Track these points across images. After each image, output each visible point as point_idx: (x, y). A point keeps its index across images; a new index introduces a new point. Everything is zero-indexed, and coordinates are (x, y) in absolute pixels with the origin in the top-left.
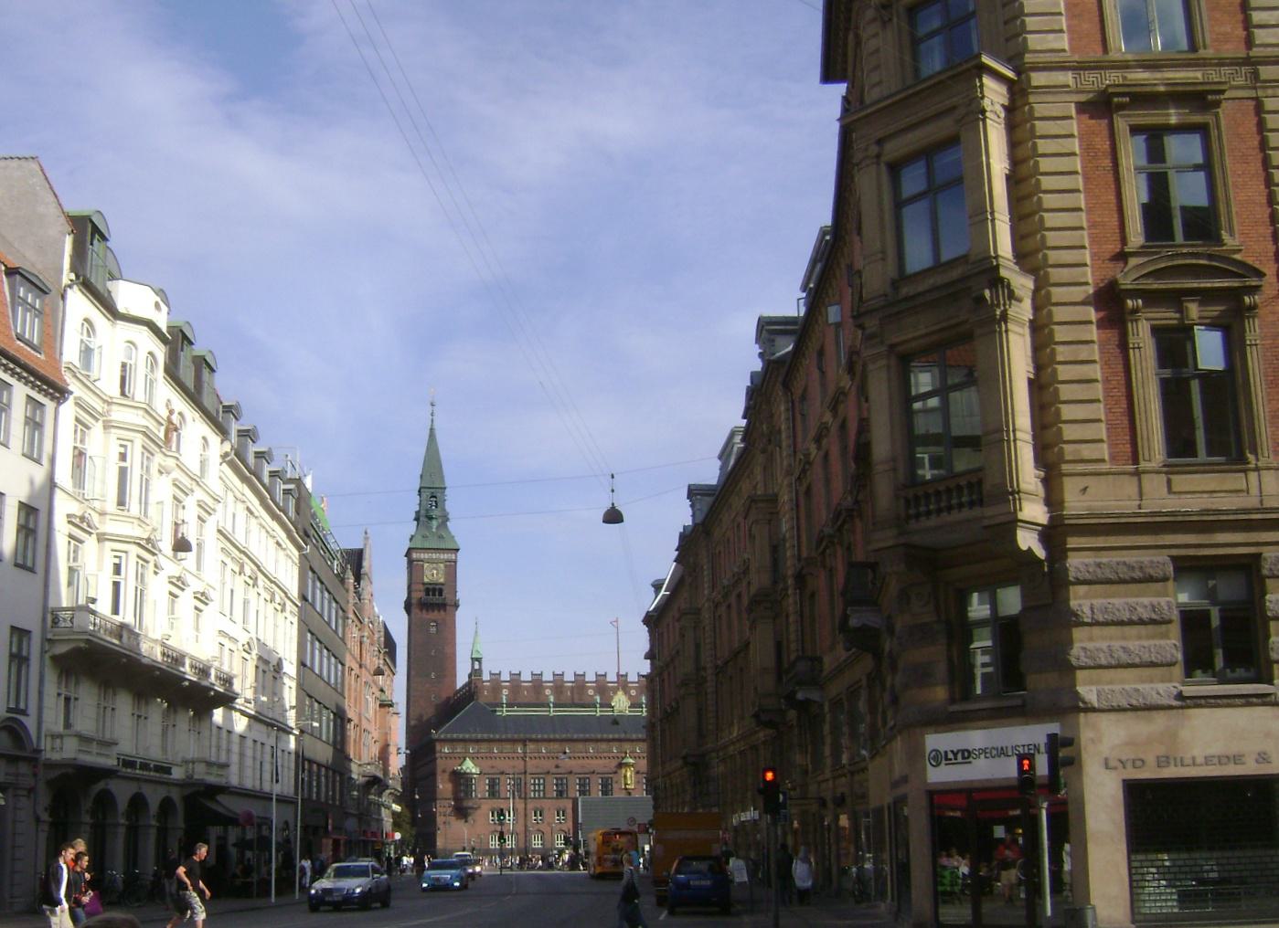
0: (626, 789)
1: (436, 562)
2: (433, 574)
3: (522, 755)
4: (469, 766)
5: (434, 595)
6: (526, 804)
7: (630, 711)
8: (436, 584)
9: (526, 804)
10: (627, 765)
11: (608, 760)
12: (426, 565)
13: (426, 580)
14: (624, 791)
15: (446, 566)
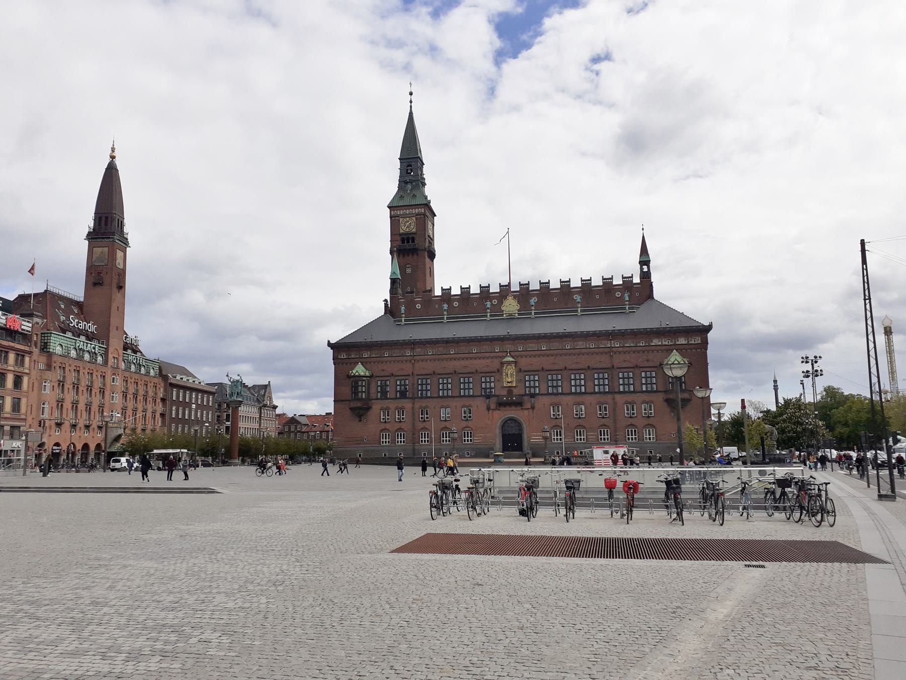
0: (508, 387)
1: (410, 216)
2: (408, 226)
3: (409, 358)
4: (360, 370)
5: (408, 242)
6: (413, 404)
7: (519, 314)
8: (410, 234)
9: (413, 404)
10: (509, 363)
11: (489, 361)
12: (401, 220)
13: (401, 231)
14: (507, 389)
15: (416, 219)
